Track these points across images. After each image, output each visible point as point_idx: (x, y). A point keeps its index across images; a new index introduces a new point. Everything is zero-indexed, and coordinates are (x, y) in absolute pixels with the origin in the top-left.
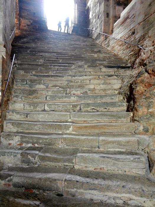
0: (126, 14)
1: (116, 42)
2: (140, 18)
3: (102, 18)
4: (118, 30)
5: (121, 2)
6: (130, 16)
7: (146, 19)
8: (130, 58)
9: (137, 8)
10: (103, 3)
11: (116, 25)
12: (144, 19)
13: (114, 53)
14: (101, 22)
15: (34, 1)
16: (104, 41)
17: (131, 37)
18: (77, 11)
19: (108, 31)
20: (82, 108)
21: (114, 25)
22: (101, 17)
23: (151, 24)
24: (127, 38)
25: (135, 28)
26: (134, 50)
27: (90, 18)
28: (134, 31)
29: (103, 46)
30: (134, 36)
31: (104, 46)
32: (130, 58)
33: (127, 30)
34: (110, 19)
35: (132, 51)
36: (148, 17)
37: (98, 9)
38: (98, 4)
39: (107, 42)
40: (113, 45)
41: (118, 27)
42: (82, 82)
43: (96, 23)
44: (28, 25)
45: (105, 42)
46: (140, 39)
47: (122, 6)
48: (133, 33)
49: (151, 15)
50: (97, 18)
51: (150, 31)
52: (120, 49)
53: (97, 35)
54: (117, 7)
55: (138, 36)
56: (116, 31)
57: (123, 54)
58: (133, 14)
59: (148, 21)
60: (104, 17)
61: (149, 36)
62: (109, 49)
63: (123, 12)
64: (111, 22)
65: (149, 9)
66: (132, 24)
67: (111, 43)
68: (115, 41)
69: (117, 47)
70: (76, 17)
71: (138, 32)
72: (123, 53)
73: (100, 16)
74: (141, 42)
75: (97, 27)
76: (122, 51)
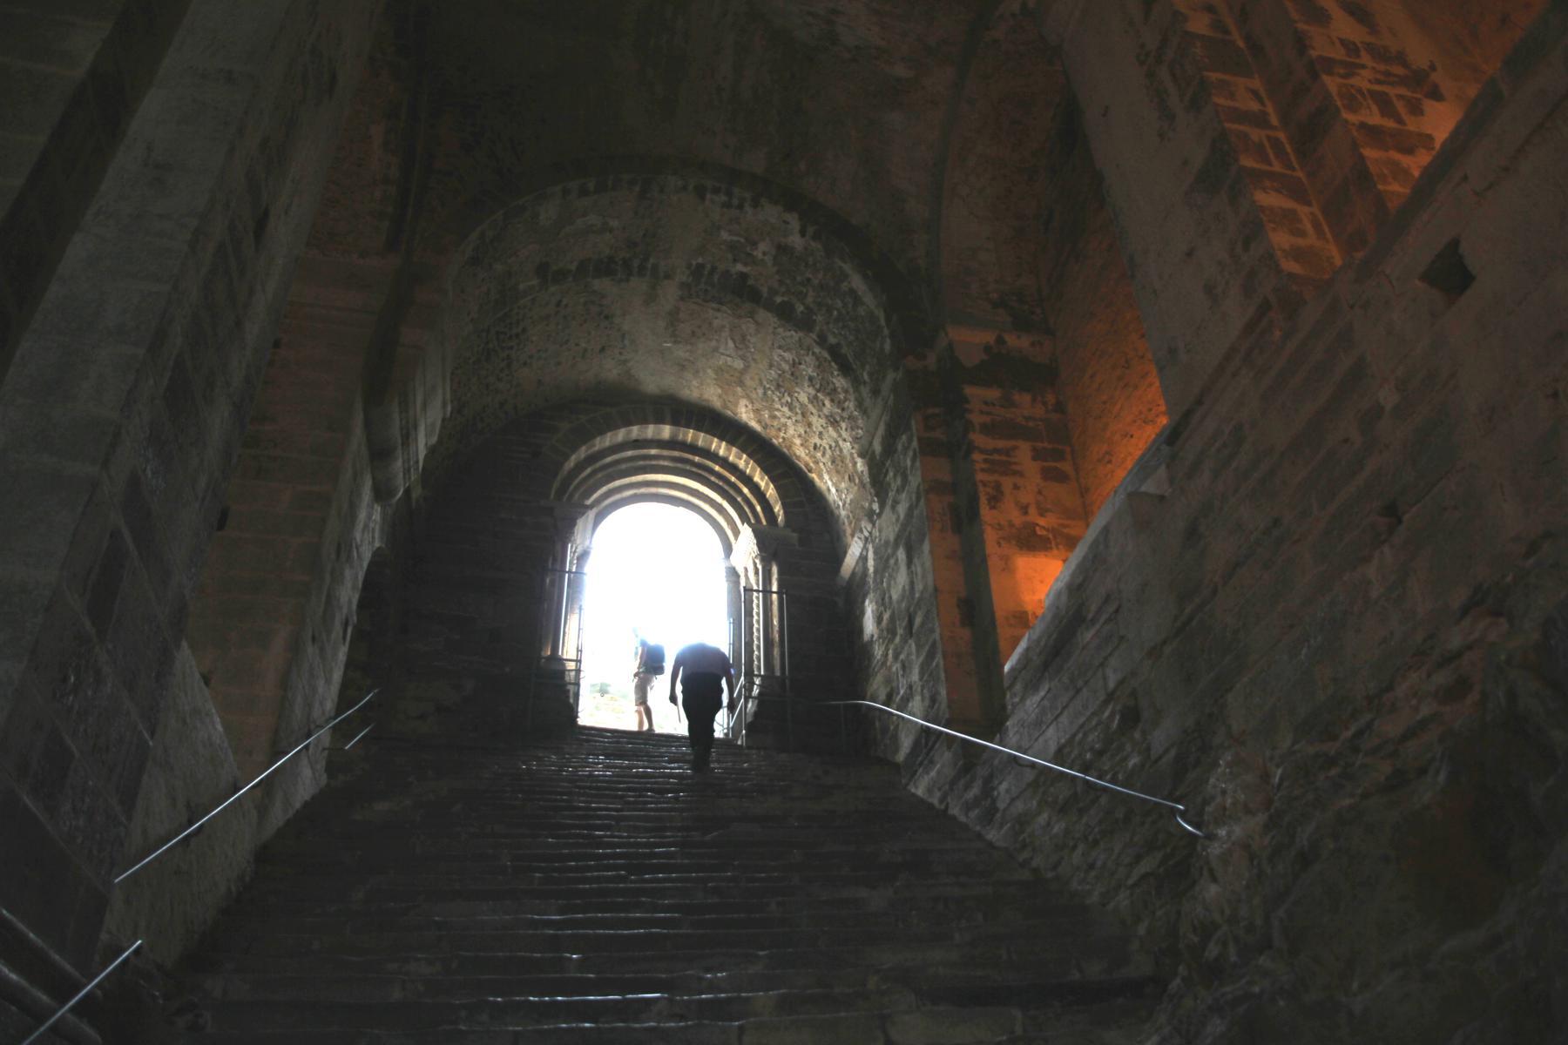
0: (1064, 598)
1: (1035, 784)
3: (932, 631)
4: (1032, 702)
6: (1093, 608)
10: (926, 547)
13: (1034, 864)
14: (931, 655)
16: (962, 782)
21: (1007, 668)
22: (923, 624)
24: (1100, 753)
27: (866, 637)
29: (954, 818)
30: (1137, 735)
31: (963, 819)
37: (902, 578)
38: (901, 554)
39: (975, 791)
40: (1020, 806)
43: (898, 665)
45: (967, 787)
47: (1055, 552)
48: (1131, 717)
49: (1215, 592)
50: (900, 631)
53: (916, 745)
55: (1162, 736)
57: (1093, 874)
68: (1030, 776)
69: (1043, 819)
70: (776, 636)
72: (1091, 866)
73: (918, 621)
75: (910, 687)
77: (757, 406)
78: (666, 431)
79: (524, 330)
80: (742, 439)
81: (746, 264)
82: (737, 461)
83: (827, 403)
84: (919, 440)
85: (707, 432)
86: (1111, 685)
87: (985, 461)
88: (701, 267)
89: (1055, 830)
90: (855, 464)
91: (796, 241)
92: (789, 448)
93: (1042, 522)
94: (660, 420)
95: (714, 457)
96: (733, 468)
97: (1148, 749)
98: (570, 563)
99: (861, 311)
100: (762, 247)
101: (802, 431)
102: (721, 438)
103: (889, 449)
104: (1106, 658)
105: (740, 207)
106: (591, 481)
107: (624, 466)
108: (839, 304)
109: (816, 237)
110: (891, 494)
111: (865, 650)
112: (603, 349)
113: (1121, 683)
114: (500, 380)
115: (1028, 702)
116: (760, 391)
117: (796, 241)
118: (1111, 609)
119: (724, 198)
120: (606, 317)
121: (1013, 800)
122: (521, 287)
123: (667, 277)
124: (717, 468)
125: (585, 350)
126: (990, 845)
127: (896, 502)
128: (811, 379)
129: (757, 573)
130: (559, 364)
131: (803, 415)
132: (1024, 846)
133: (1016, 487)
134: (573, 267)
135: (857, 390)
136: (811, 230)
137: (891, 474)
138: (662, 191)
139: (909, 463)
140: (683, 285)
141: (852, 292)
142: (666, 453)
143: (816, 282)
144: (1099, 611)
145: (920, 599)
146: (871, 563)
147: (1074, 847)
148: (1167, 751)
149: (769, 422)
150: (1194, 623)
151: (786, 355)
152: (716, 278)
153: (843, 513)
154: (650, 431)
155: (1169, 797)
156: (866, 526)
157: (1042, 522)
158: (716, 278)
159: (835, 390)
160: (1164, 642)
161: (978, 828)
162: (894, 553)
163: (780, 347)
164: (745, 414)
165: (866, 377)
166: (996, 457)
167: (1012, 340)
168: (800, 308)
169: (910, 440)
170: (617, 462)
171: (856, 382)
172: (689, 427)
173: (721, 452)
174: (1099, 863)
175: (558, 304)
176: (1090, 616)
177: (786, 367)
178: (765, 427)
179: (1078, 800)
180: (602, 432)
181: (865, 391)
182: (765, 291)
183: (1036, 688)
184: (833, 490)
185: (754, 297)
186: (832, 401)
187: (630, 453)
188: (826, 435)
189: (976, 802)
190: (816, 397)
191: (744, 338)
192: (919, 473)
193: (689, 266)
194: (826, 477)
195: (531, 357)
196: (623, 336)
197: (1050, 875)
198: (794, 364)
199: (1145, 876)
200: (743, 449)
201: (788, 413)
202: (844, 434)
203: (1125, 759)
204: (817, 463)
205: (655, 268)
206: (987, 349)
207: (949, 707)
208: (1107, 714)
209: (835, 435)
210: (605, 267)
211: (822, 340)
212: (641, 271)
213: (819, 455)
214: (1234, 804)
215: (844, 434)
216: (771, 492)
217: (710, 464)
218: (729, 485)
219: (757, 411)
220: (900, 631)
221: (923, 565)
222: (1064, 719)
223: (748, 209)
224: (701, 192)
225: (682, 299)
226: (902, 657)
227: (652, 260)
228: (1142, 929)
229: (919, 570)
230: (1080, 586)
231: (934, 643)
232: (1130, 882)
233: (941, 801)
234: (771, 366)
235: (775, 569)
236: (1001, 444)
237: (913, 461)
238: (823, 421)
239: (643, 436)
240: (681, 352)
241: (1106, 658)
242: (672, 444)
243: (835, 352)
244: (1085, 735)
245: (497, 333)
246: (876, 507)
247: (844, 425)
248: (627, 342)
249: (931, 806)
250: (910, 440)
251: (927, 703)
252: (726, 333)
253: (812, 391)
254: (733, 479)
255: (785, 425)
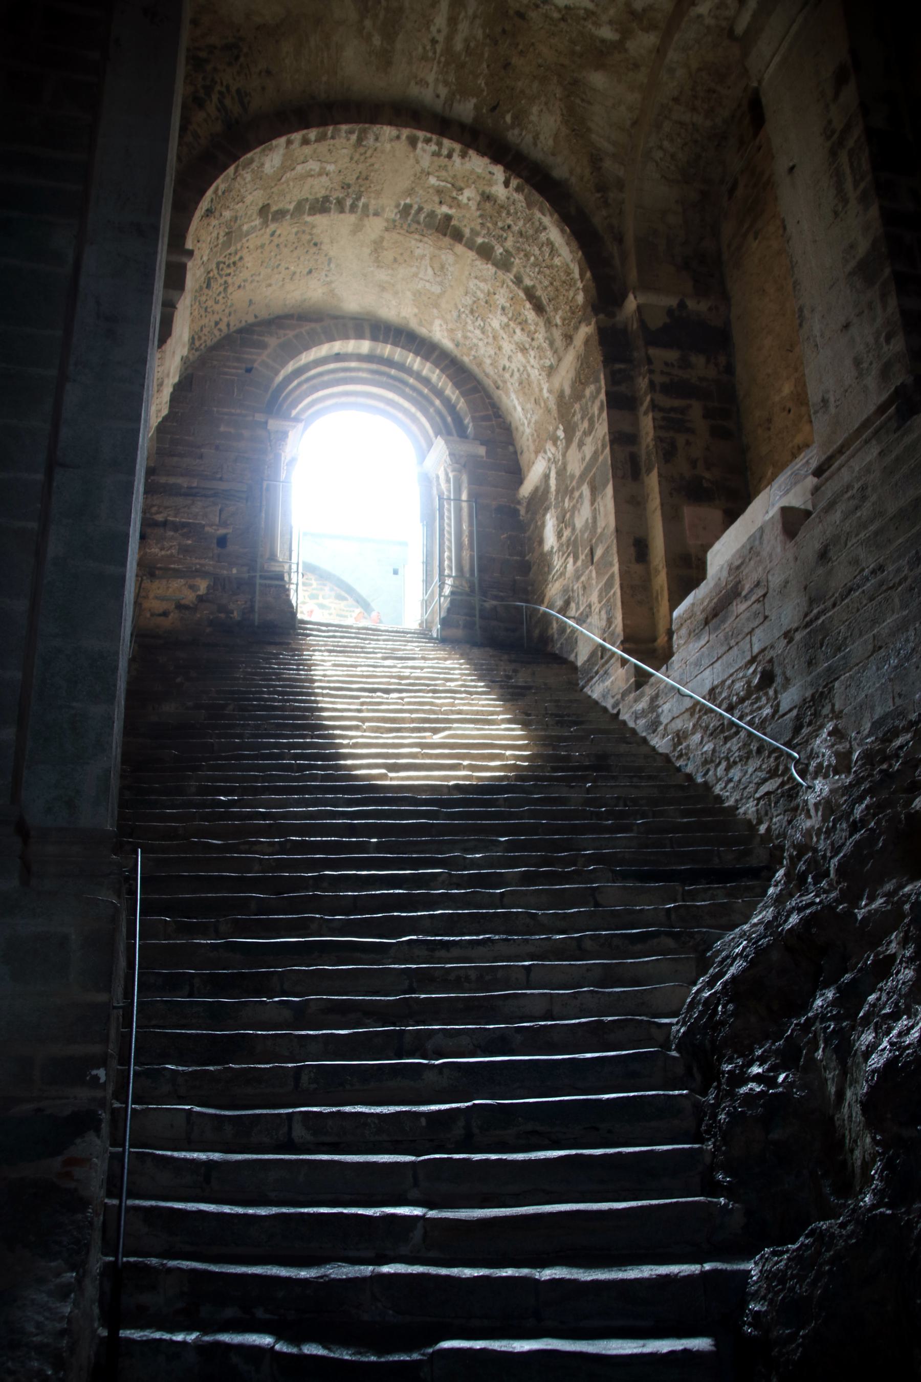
0: (725, 574)
2: (788, 613)
3: (611, 564)
5: (705, 484)
6: (747, 587)
7: (817, 617)
8: (766, 814)
9: (770, 555)
10: (609, 490)
11: (683, 621)
12: (806, 615)
14: (609, 585)
15: (221, 479)
16: (632, 695)
17: (758, 699)
18: (470, 508)
19: (648, 644)
20: (476, 1131)
21: (676, 614)
23: (839, 649)
25: (772, 653)
26: (781, 768)
27: (547, 547)
28: (768, 668)
29: (624, 723)
30: (771, 692)
31: (631, 724)
32: (766, 814)
33: (738, 657)
34: (657, 570)
35: (773, 773)
36: (823, 612)
38: (585, 490)
39: (642, 705)
40: (678, 725)
41: (695, 634)
42: (488, 978)
43: (580, 585)
44: (180, 607)
45: (636, 700)
46: (798, 717)
48: (767, 678)
49: (834, 605)
50: (582, 557)
51: (837, 684)
52: (714, 750)
53: (593, 654)
54: (689, 512)
55: (789, 698)
56: (686, 651)
57: (731, 785)
58: (755, 577)
59: (824, 630)
60: (621, 562)
61: (837, 707)
62: (660, 743)
63: (717, 546)
64: (662, 590)
65: (821, 571)
66: (758, 632)
67: (668, 708)
68: (688, 703)
69: (697, 737)
70: (466, 541)
71: (787, 680)
72: (730, 780)
73: (599, 553)
74: (805, 731)
75: (590, 606)
76: (724, 765)
77: (450, 326)
78: (365, 346)
79: (241, 258)
80: (434, 356)
81: (451, 207)
82: (430, 375)
83: (518, 331)
84: (607, 394)
85: (403, 347)
86: (756, 650)
87: (664, 419)
88: (408, 207)
89: (705, 749)
90: (541, 390)
91: (499, 191)
92: (480, 365)
93: (707, 475)
94: (360, 336)
95: (409, 371)
96: (426, 381)
97: (778, 705)
98: (283, 476)
99: (557, 261)
100: (467, 193)
101: (492, 352)
102: (417, 353)
103: (577, 396)
104: (753, 629)
105: (449, 156)
106: (298, 392)
107: (326, 378)
108: (537, 252)
109: (518, 189)
110: (578, 434)
111: (545, 561)
112: (310, 272)
113: (763, 650)
114: (217, 302)
115: (691, 645)
116: (455, 314)
117: (499, 191)
118: (760, 592)
119: (434, 148)
120: (316, 244)
121: (673, 718)
122: (245, 228)
123: (376, 214)
124: (411, 380)
125: (294, 273)
126: (654, 749)
127: (581, 444)
128: (503, 309)
129: (448, 481)
130: (270, 285)
131: (495, 338)
132: (680, 756)
133: (688, 443)
134: (291, 207)
135: (548, 329)
136: (514, 182)
137: (578, 417)
138: (377, 139)
139: (596, 412)
140: (387, 220)
141: (550, 243)
142: (365, 365)
143: (515, 229)
144: (751, 591)
145: (602, 534)
146: (553, 482)
147: (720, 763)
148: (791, 710)
149: (461, 341)
150: (820, 621)
151: (482, 285)
152: (422, 217)
153: (528, 431)
154: (351, 346)
155: (788, 744)
156: (549, 446)
157: (707, 475)
158: (422, 217)
159: (526, 321)
160: (797, 630)
161: (644, 734)
162: (579, 486)
163: (476, 278)
164: (439, 333)
165: (558, 321)
166: (672, 415)
167: (691, 304)
168: (499, 250)
169: (598, 391)
170: (321, 374)
171: (549, 323)
172: (385, 341)
173: (416, 367)
174: (736, 778)
175: (273, 234)
176: (744, 593)
177: (481, 296)
178: (457, 345)
179: (725, 731)
180: (307, 348)
181: (557, 334)
182: (467, 232)
183: (698, 636)
184: (519, 409)
185: (458, 236)
186: (523, 330)
187: (332, 366)
188: (514, 359)
189: (644, 714)
190: (507, 325)
191: (442, 267)
192: (606, 424)
193: (397, 206)
194: (513, 396)
195: (245, 281)
196: (330, 260)
197: (700, 780)
198: (489, 294)
199: (768, 794)
200: (436, 364)
201: (481, 336)
202: (532, 360)
203: (760, 708)
204: (505, 382)
205: (366, 206)
206: (670, 312)
207: (624, 630)
208: (751, 670)
209: (523, 360)
210: (321, 206)
211: (518, 280)
212: (353, 208)
213: (507, 375)
214: (829, 766)
215: (532, 360)
216: (462, 405)
217: (404, 376)
218: (422, 395)
219: (451, 331)
220: (582, 557)
221: (605, 506)
222: (716, 665)
223: (456, 157)
224: (413, 142)
225: (387, 229)
226: (583, 578)
227: (363, 200)
228: (762, 829)
229: (602, 509)
230: (738, 567)
231: (612, 576)
232: (757, 795)
233: (614, 707)
234: (466, 293)
235: (465, 478)
236: (677, 403)
237: (601, 409)
238: (513, 347)
239: (343, 351)
240: (382, 275)
241: (753, 629)
242: (369, 358)
243: (530, 294)
244: (733, 682)
245: (218, 264)
246: (561, 434)
247: (532, 353)
248: (332, 266)
249: (605, 710)
250: (598, 391)
251: (604, 623)
252: (427, 261)
253: (505, 320)
254: (426, 391)
255: (476, 345)
